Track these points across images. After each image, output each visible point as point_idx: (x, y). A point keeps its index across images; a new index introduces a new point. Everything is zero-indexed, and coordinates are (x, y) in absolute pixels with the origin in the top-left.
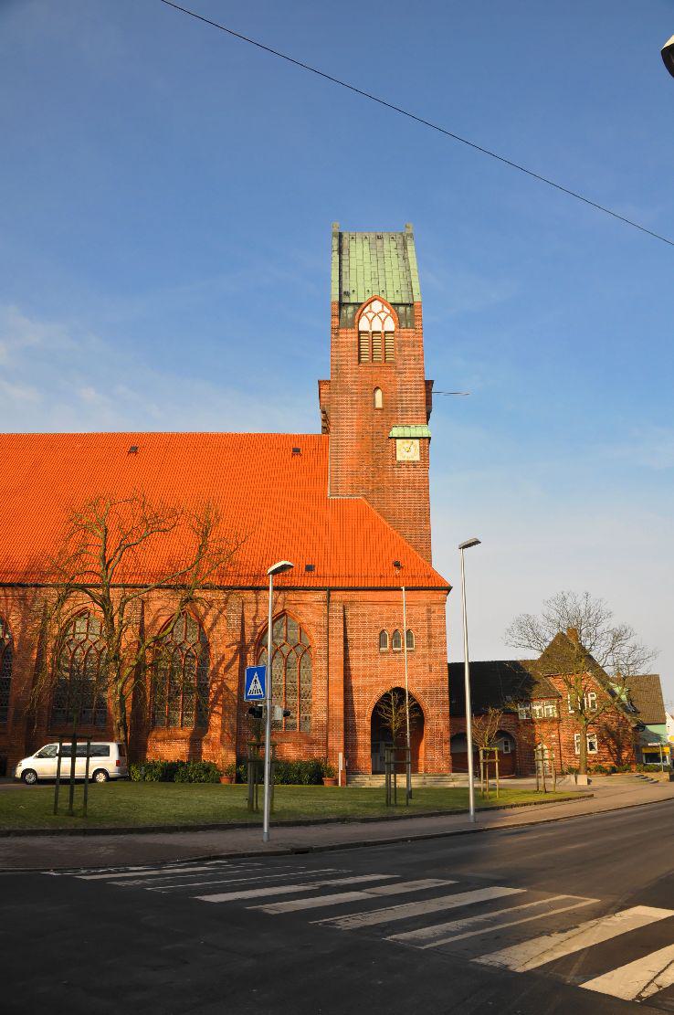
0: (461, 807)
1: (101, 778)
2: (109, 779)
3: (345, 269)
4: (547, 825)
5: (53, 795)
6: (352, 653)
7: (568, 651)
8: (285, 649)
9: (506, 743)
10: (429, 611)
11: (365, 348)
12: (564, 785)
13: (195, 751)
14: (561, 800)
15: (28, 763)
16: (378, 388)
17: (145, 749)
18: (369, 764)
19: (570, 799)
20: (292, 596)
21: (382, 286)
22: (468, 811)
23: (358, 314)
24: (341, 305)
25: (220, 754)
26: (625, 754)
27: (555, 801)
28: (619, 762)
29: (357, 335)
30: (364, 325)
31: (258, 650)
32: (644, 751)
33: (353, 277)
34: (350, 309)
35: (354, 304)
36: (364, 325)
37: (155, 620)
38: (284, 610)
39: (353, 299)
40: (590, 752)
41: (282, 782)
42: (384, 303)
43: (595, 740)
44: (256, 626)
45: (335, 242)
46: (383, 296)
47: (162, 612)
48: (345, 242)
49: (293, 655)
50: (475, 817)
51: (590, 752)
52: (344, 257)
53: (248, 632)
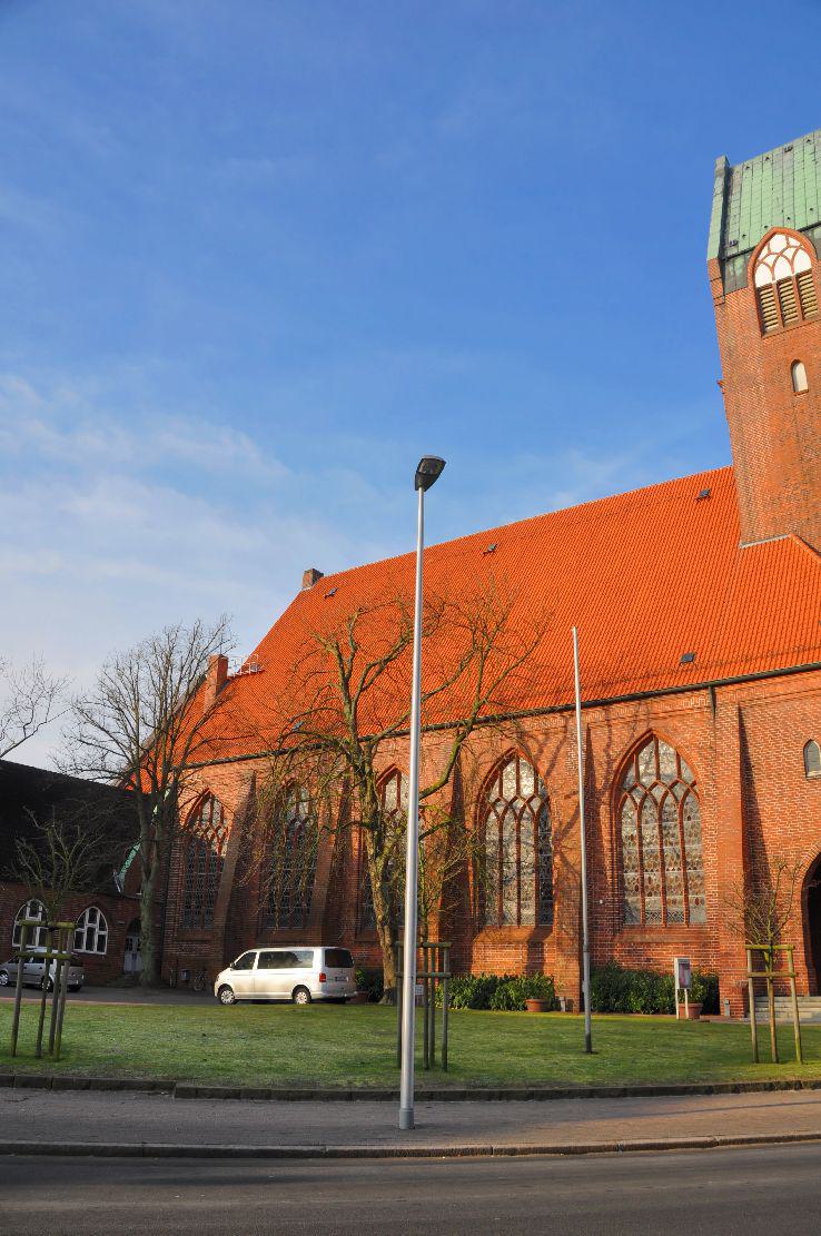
0: (386, 1084)
1: (302, 998)
2: (311, 1001)
3: (733, 210)
4: (782, 1152)
5: (450, 1025)
6: (762, 786)
8: (658, 793)
11: (771, 310)
13: (535, 963)
15: (227, 976)
16: (796, 362)
17: (470, 959)
18: (803, 980)
20: (660, 706)
21: (787, 213)
22: (394, 1096)
23: (751, 264)
24: (723, 260)
25: (563, 970)
29: (751, 297)
30: (763, 277)
31: (617, 799)
33: (745, 219)
34: (739, 262)
35: (744, 253)
36: (763, 277)
37: (475, 772)
38: (650, 730)
39: (743, 246)
41: (644, 1009)
42: (788, 233)
44: (609, 763)
45: (719, 184)
46: (789, 225)
47: (481, 760)
48: (736, 177)
49: (670, 799)
50: (410, 1114)
52: (733, 198)
53: (600, 773)
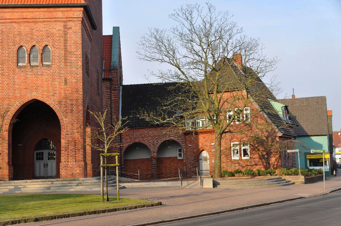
7: (236, 74)
9: (180, 151)
10: (65, 27)
12: (190, 188)
14: (80, 215)
19: (144, 206)
26: (273, 160)
27: (104, 212)
28: (267, 165)
32: (309, 157)
40: (243, 158)
43: (247, 147)
51: (243, 158)
